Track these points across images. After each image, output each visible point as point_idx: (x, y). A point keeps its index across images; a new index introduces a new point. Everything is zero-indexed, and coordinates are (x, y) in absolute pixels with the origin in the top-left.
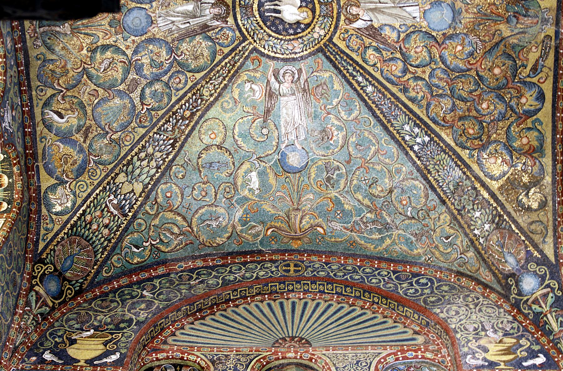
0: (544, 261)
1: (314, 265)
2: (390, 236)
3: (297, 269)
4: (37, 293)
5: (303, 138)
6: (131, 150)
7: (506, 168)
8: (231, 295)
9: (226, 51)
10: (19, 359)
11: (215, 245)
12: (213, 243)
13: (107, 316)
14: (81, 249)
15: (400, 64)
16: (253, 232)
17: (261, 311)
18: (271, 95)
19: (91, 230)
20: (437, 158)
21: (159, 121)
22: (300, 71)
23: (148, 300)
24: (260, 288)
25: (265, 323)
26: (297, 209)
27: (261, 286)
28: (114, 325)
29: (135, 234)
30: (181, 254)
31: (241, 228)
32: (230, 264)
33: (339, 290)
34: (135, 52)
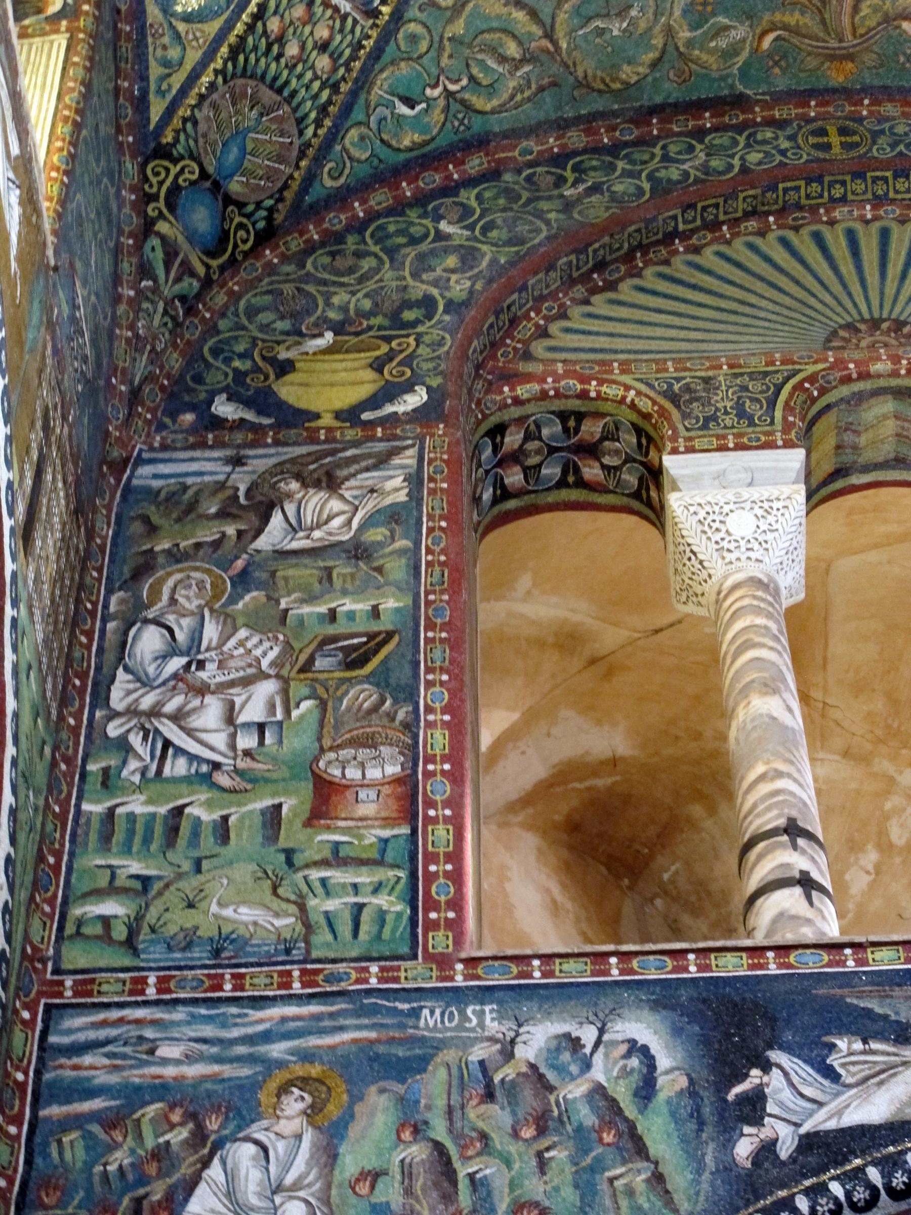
1: (891, 128)
3: (849, 139)
4: (163, 238)
8: (680, 219)
10: (149, 423)
11: (617, 86)
12: (613, 80)
13: (360, 295)
14: (261, 115)
17: (768, 260)
19: (283, 61)
23: (461, 246)
24: (755, 197)
25: (787, 289)
27: (759, 191)
28: (385, 315)
29: (403, 64)
31: (688, 34)
32: (659, 137)
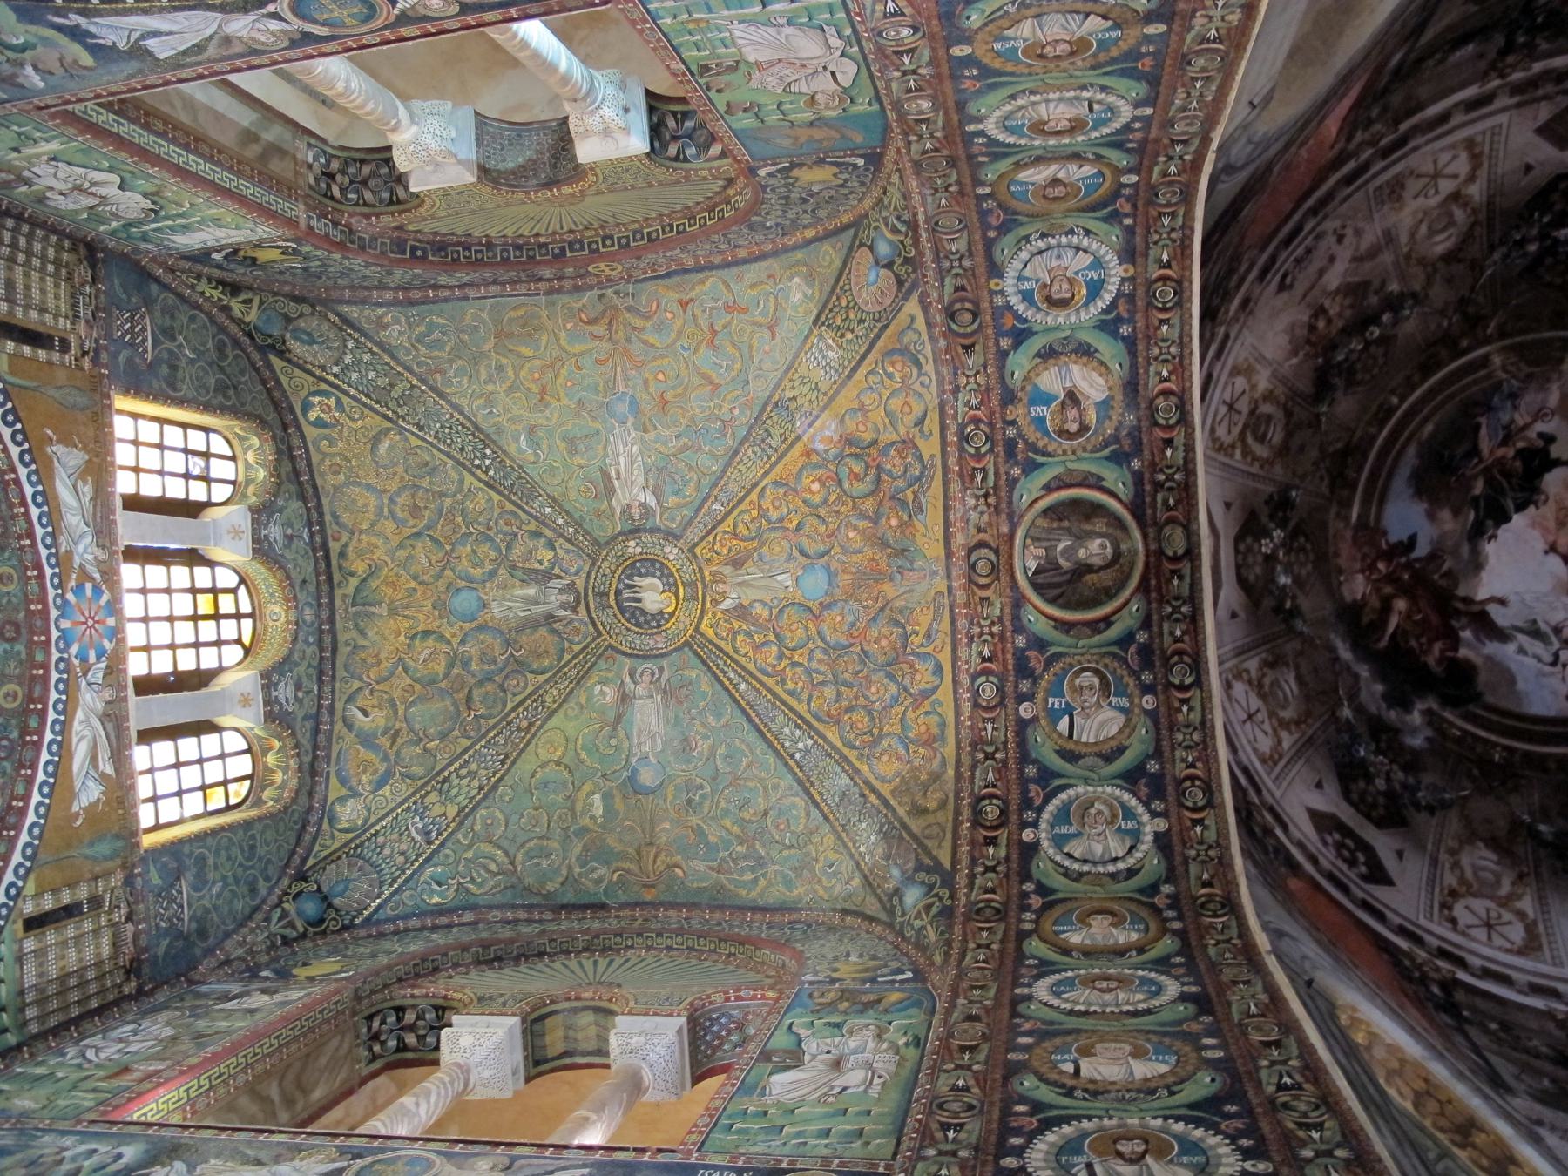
0: (937, 867)
2: (764, 875)
5: (659, 748)
6: (450, 764)
7: (896, 765)
9: (577, 648)
15: (774, 649)
16: (595, 876)
18: (624, 698)
20: (821, 765)
21: (488, 731)
22: (661, 670)
26: (651, 844)
30: (498, 899)
33: (690, 943)
34: (463, 642)
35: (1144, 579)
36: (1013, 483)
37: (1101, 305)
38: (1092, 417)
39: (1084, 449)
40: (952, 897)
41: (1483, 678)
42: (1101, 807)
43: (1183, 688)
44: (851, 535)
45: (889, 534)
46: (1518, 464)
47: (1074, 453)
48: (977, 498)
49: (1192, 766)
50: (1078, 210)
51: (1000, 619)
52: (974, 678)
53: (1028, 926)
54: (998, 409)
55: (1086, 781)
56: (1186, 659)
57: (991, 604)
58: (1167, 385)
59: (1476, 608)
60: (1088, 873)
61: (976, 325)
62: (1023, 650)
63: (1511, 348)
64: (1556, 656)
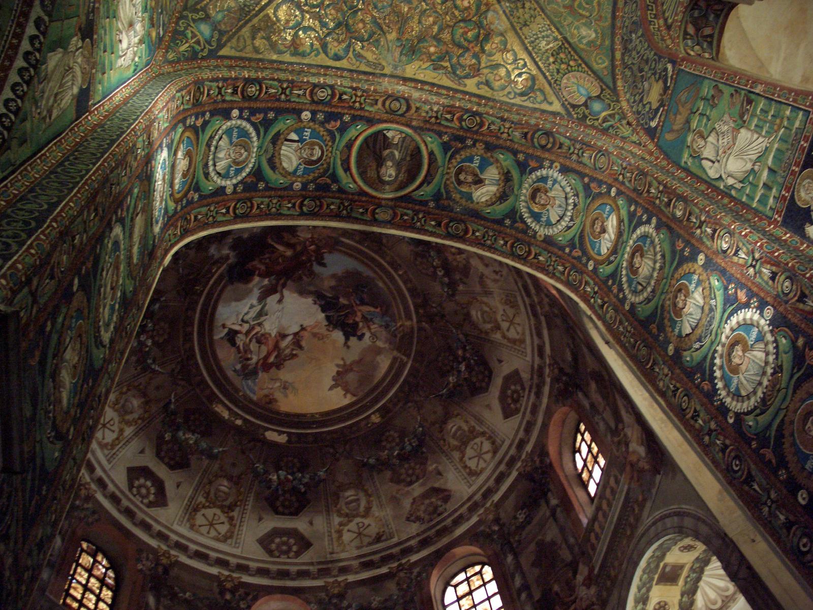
0: (220, 46)
35: (366, 194)
36: (440, 134)
37: (526, 215)
38: (464, 189)
39: (447, 179)
40: (203, 58)
41: (241, 286)
42: (244, 156)
43: (301, 205)
44: (431, 19)
45: (426, 44)
46: (351, 321)
47: (448, 173)
48: (437, 112)
49: (258, 207)
50: (583, 231)
51: (362, 109)
52: (332, 87)
53: (188, 121)
54: (485, 139)
55: (260, 147)
56: (317, 209)
57: (372, 105)
58: (471, 233)
59: (279, 288)
60: (210, 151)
61: (536, 144)
62: (341, 119)
63: (412, 332)
64: (247, 322)
